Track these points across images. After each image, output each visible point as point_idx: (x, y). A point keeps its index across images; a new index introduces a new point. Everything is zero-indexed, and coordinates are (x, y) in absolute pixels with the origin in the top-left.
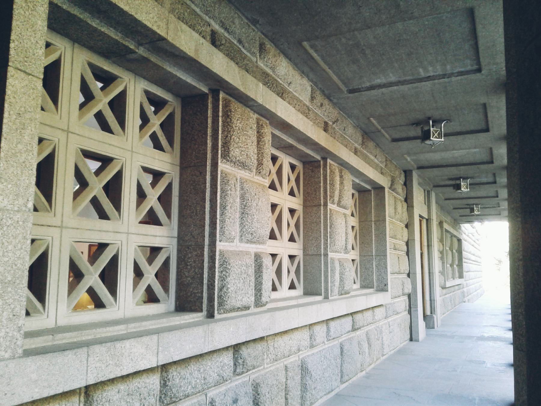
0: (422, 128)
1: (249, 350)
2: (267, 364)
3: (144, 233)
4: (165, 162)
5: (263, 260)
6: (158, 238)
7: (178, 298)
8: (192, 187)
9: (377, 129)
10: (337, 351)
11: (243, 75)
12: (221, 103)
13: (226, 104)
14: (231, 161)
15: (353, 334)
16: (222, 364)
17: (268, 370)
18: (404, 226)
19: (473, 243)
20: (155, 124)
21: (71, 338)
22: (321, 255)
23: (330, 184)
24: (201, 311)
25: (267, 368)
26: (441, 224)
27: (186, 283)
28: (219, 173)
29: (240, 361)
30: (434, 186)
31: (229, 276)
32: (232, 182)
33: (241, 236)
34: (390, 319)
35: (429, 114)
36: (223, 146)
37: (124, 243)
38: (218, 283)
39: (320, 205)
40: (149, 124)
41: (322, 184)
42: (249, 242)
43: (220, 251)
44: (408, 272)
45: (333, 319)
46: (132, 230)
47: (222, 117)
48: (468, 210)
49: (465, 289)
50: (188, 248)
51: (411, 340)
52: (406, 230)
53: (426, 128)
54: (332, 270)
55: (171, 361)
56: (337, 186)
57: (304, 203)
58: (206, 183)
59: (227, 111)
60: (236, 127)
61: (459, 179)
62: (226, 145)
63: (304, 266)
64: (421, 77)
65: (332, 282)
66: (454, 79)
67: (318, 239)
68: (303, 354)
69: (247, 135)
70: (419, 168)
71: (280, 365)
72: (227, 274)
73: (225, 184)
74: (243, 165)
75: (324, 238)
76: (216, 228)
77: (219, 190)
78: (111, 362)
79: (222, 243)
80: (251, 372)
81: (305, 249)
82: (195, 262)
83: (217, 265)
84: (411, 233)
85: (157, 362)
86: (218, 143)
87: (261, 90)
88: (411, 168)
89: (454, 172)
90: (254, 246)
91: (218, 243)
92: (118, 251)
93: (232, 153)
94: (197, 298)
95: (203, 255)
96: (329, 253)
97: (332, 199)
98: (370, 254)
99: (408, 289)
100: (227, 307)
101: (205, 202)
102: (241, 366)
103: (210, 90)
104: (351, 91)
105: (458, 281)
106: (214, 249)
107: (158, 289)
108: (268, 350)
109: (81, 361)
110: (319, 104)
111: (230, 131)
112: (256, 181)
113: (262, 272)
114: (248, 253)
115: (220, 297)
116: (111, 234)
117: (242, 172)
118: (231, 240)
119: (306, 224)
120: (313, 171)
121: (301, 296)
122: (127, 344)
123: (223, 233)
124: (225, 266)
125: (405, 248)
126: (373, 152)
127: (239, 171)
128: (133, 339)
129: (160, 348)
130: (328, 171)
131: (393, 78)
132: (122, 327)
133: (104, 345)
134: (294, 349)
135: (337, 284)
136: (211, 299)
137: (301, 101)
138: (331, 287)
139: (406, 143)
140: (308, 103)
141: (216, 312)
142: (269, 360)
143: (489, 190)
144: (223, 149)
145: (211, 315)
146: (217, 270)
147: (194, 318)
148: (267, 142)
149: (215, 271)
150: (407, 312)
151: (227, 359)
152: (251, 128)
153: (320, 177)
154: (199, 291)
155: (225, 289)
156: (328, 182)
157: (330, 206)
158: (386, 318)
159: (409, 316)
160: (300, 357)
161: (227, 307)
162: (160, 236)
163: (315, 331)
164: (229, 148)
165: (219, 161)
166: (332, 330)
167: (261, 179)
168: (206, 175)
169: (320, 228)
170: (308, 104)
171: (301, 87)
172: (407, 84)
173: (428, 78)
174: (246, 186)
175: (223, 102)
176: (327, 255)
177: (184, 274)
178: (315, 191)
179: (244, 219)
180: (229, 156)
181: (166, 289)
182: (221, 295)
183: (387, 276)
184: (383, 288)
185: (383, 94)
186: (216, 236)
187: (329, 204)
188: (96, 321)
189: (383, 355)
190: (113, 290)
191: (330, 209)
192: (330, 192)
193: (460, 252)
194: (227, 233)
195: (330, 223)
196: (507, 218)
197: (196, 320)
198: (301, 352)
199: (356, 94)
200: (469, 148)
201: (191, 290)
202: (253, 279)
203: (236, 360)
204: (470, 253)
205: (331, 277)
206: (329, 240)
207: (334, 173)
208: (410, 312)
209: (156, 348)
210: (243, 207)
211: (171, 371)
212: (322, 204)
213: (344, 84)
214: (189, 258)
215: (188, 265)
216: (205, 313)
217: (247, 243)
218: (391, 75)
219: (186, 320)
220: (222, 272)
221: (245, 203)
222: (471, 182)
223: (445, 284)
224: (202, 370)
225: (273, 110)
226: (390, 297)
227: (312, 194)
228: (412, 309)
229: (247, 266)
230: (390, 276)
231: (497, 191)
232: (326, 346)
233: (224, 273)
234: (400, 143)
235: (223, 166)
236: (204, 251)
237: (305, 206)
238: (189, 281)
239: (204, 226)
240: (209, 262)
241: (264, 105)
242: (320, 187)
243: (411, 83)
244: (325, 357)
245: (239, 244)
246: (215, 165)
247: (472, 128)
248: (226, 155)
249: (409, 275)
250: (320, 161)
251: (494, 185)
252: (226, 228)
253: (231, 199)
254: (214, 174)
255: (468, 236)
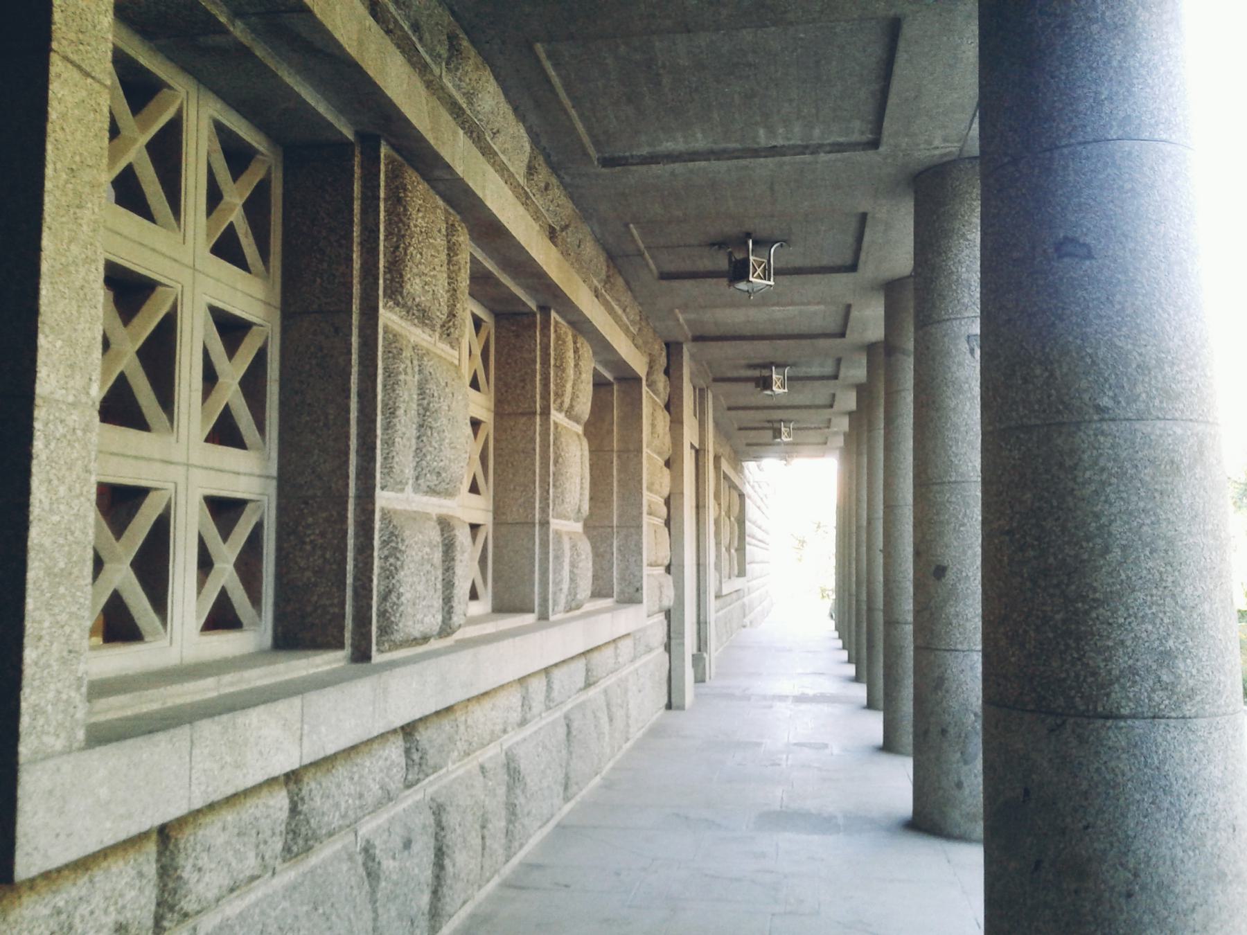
0: (730, 254)
1: (429, 732)
2: (454, 763)
3: (217, 465)
4: (248, 295)
5: (457, 532)
6: (243, 479)
7: (280, 618)
8: (314, 362)
9: (639, 250)
10: (562, 731)
11: (433, 108)
12: (382, 167)
13: (393, 171)
14: (403, 306)
15: (583, 697)
16: (388, 763)
17: (453, 776)
18: (661, 462)
19: (759, 503)
20: (235, 205)
21: (123, 707)
22: (534, 524)
23: (555, 365)
24: (341, 646)
25: (453, 772)
26: (717, 459)
27: (300, 584)
28: (380, 331)
29: (416, 757)
30: (716, 380)
31: (402, 567)
32: (407, 353)
33: (417, 478)
34: (638, 664)
35: (748, 226)
36: (389, 270)
37: (181, 488)
38: (379, 584)
39: (535, 413)
40: (222, 206)
41: (538, 366)
42: (432, 491)
43: (382, 509)
44: (667, 562)
45: (556, 665)
46: (196, 458)
47: (386, 200)
48: (770, 433)
49: (746, 600)
50: (306, 503)
51: (669, 706)
52: (666, 471)
53: (739, 256)
54: (557, 557)
55: (321, 755)
56: (571, 371)
57: (496, 405)
58: (349, 353)
59: (397, 187)
60: (416, 226)
61: (768, 366)
62: (396, 267)
63: (495, 546)
64: (756, 146)
65: (557, 583)
66: (823, 157)
67: (528, 487)
68: (510, 740)
69: (434, 247)
70: (698, 339)
71: (472, 764)
72: (399, 563)
73: (394, 358)
74: (423, 317)
75: (541, 487)
76: (373, 459)
77: (380, 371)
78: (228, 759)
79: (386, 494)
80: (427, 780)
81: (498, 511)
82: (323, 535)
83: (377, 543)
84: (677, 479)
85: (301, 758)
86: (378, 262)
87: (461, 144)
88: (681, 339)
89: (763, 350)
90: (434, 500)
91: (378, 492)
92: (168, 507)
93: (408, 286)
94: (328, 617)
95: (344, 519)
96: (552, 521)
97: (559, 401)
98: (607, 523)
99: (668, 601)
100: (398, 637)
101: (348, 397)
102: (416, 768)
103: (357, 133)
104: (608, 162)
105: (738, 583)
106: (370, 507)
107: (239, 597)
108: (457, 732)
109: (180, 758)
110: (543, 185)
111: (404, 236)
112: (438, 352)
113: (453, 559)
114: (427, 516)
115: (383, 614)
116: (158, 465)
117: (418, 331)
118: (400, 486)
119: (500, 455)
120: (517, 336)
121: (487, 615)
122: (254, 716)
123: (389, 470)
124: (393, 544)
125: (665, 510)
126: (623, 299)
127: (413, 329)
128: (262, 707)
129: (306, 727)
130: (553, 336)
131: (700, 142)
132: (210, 682)
133: (216, 718)
134: (499, 728)
135: (565, 586)
136: (362, 620)
137: (512, 175)
138: (555, 593)
139: (688, 284)
140: (522, 180)
141: (374, 648)
142: (456, 753)
143: (819, 393)
144: (388, 276)
145: (361, 655)
146: (376, 554)
147: (329, 663)
148: (463, 262)
149: (372, 556)
150: (662, 649)
151: (394, 751)
152: (439, 231)
153: (535, 351)
154: (336, 601)
155: (393, 597)
156: (552, 362)
157: (556, 416)
158: (633, 660)
159: (667, 656)
160: (505, 747)
161: (398, 637)
162: (245, 474)
163: (531, 690)
164: (401, 276)
165: (381, 304)
166: (556, 686)
167: (447, 348)
168: (350, 335)
169: (534, 464)
170: (521, 182)
171: (514, 141)
172: (728, 159)
173: (773, 151)
174: (429, 364)
175: (386, 165)
176: (548, 523)
177: (296, 563)
178: (523, 380)
179: (425, 439)
180: (401, 294)
181: (255, 599)
182: (386, 611)
183: (641, 570)
184: (632, 597)
185: (672, 173)
186: (374, 477)
187: (553, 411)
188: (130, 672)
189: (627, 739)
190: (159, 601)
191: (555, 423)
192: (556, 385)
193: (741, 521)
194: (397, 469)
195: (555, 453)
196: (837, 452)
197: (335, 666)
198: (506, 737)
199: (618, 168)
200: (809, 303)
201: (315, 598)
202: (439, 572)
203: (407, 752)
204: (754, 523)
205: (554, 573)
206: (551, 491)
207: (564, 342)
208: (668, 647)
209: (299, 725)
210: (422, 411)
211: (306, 780)
212: (538, 410)
213: (596, 143)
214: (308, 526)
215: (304, 543)
216: (347, 651)
217: (426, 493)
218: (699, 136)
219: (318, 666)
220: (386, 558)
221: (425, 402)
222: (792, 374)
223: (720, 589)
224: (356, 777)
225: (480, 194)
226: (645, 615)
227: (516, 386)
228: (673, 642)
229: (432, 546)
230: (646, 570)
231: (834, 395)
232: (544, 722)
233: (392, 560)
234: (676, 284)
235: (388, 317)
236: (346, 510)
237: (499, 414)
238: (309, 579)
239: (347, 454)
240: (357, 536)
241: (466, 179)
242: (534, 371)
243: (738, 158)
244: (544, 747)
245: (413, 495)
246: (370, 314)
247: (825, 262)
248: (395, 290)
249: (668, 569)
250: (534, 314)
251: (832, 382)
252: (396, 459)
253: (406, 393)
254: (369, 332)
255: (753, 487)
